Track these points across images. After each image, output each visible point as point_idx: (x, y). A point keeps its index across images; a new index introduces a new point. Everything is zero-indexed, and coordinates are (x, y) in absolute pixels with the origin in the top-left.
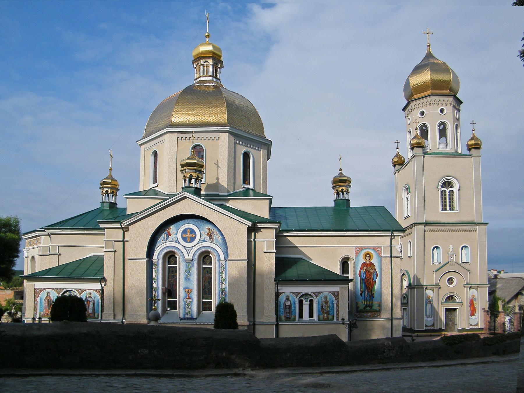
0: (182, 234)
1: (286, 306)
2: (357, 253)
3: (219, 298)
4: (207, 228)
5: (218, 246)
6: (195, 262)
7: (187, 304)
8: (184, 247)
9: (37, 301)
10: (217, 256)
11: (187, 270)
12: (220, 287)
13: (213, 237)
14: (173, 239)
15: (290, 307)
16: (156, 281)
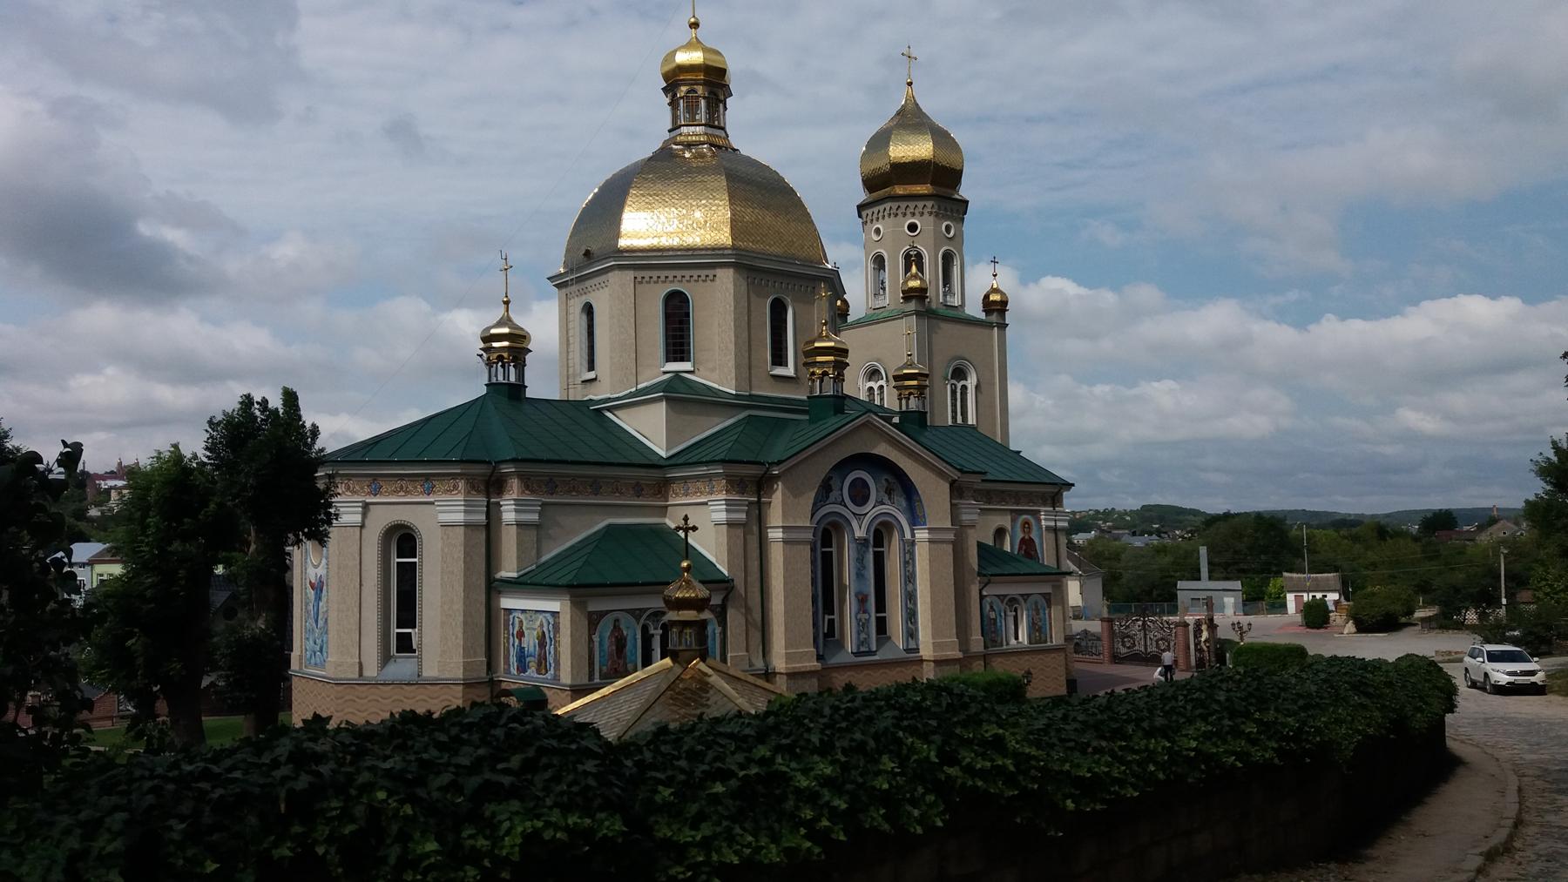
1: (991, 619)
2: (1014, 521)
8: (853, 513)
9: (593, 642)
12: (906, 589)
15: (995, 620)
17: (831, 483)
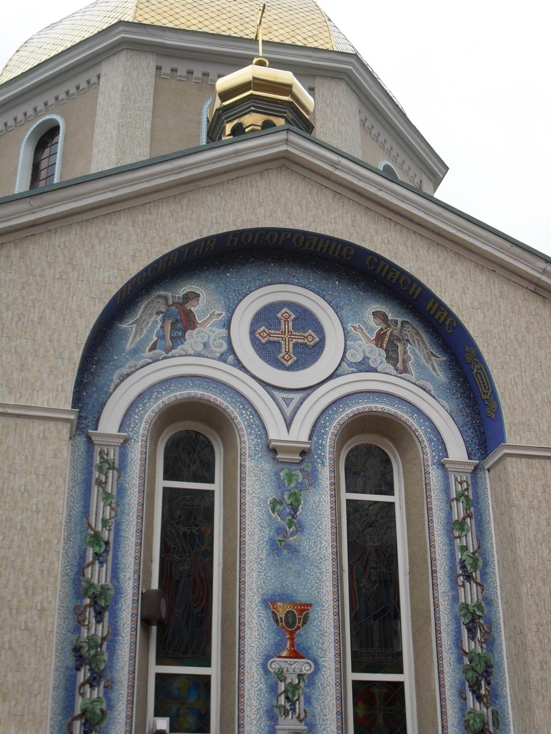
0: (252, 325)
3: (460, 660)
4: (374, 314)
5: (434, 397)
6: (323, 464)
7: (282, 687)
10: (430, 440)
11: (281, 503)
13: (405, 353)
14: (205, 345)
16: (106, 551)
17: (195, 309)
